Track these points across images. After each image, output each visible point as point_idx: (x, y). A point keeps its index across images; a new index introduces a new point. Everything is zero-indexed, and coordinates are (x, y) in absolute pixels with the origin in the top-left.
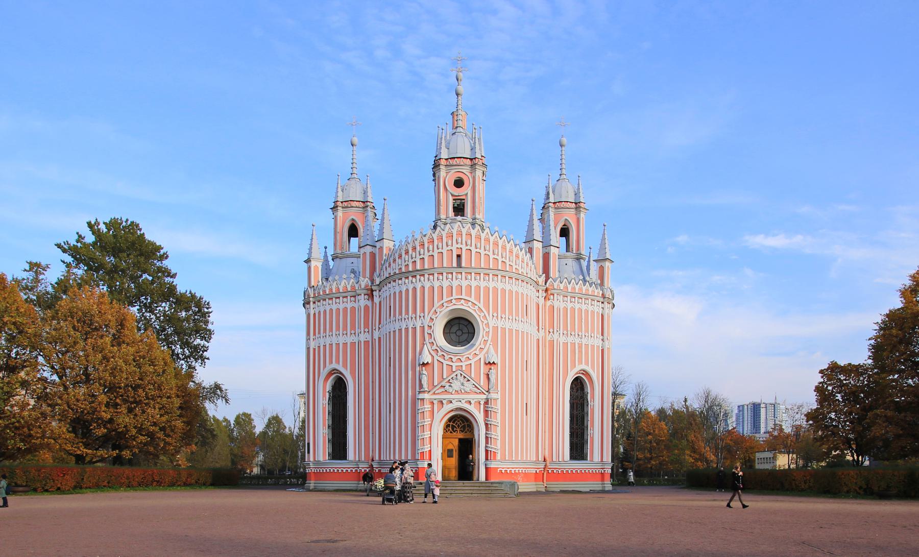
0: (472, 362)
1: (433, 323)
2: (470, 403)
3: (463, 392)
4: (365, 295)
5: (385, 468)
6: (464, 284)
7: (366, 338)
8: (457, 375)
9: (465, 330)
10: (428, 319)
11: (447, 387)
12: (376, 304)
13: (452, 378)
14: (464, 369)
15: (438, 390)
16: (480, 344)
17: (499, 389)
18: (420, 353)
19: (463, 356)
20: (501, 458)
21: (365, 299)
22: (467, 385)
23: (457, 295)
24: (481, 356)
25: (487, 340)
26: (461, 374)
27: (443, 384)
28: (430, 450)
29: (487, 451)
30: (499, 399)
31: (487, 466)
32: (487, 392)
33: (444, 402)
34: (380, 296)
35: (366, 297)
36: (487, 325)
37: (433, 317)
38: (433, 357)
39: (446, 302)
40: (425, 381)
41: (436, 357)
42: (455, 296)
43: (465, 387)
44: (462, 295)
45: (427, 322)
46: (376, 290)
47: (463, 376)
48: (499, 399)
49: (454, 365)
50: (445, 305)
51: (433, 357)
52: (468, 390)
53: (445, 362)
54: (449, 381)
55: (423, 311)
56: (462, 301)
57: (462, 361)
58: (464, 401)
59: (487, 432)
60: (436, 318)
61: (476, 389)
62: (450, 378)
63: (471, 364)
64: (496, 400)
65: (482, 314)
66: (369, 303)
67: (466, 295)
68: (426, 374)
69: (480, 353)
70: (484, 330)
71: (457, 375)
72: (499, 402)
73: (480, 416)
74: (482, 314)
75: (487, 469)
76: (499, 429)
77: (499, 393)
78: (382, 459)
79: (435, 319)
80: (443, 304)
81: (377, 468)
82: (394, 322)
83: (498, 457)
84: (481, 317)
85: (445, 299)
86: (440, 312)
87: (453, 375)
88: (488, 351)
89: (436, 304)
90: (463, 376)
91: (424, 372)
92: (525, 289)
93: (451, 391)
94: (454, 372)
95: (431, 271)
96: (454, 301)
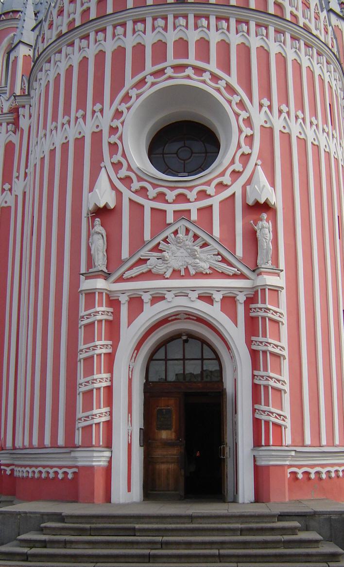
0: (215, 202)
1: (121, 120)
2: (208, 299)
3: (192, 272)
4: (8, 124)
5: (21, 466)
6: (193, 36)
7: (6, 202)
8: (176, 232)
9: (197, 146)
10: (109, 112)
11: (153, 262)
12: (22, 130)
13: (165, 240)
14: (194, 216)
15: (131, 268)
16: (233, 162)
17: (282, 265)
18: (91, 189)
19: (191, 188)
20: (293, 440)
21: (7, 132)
22: (203, 256)
23: (176, 57)
24: (236, 188)
25: (249, 155)
26: (187, 231)
27: (143, 253)
28: (109, 424)
29: (257, 422)
30: (284, 291)
31: (258, 463)
32: (254, 271)
33: (146, 298)
34: (30, 116)
35: (10, 127)
36: (248, 122)
37: (123, 107)
38: (119, 194)
39: (152, 74)
40: (100, 248)
41: (127, 195)
42: (171, 60)
43: (198, 261)
44: (187, 57)
45: (105, 122)
46: (24, 107)
47: (191, 234)
48: (284, 291)
49: (170, 209)
50: (150, 80)
51: (119, 194)
52: (205, 266)
53: (148, 205)
54: (156, 249)
55: (99, 97)
56: (189, 71)
57: (188, 201)
58: (194, 295)
59: (256, 373)
60: (128, 109)
61: (224, 265)
62: (159, 239)
63: (211, 207)
64: (275, 290)
65: (236, 99)
66: (15, 139)
67: (198, 58)
68: (104, 232)
69: (233, 182)
70: (240, 131)
71: (176, 232)
72: (283, 295)
73: (236, 333)
74: (236, 99)
75: (256, 468)
76: (285, 365)
77: (283, 274)
78: (16, 445)
79: (125, 111)
80: (145, 78)
81: (8, 465)
82: (44, 139)
83: (288, 438)
84: (234, 104)
85: (149, 68)
86: (138, 96)
87: (169, 232)
88: (249, 182)
89: (129, 81)
90: (191, 234)
91: (99, 228)
92: (325, 70)
93: (161, 272)
94: (169, 224)
95: (119, 17)
96: (169, 72)
